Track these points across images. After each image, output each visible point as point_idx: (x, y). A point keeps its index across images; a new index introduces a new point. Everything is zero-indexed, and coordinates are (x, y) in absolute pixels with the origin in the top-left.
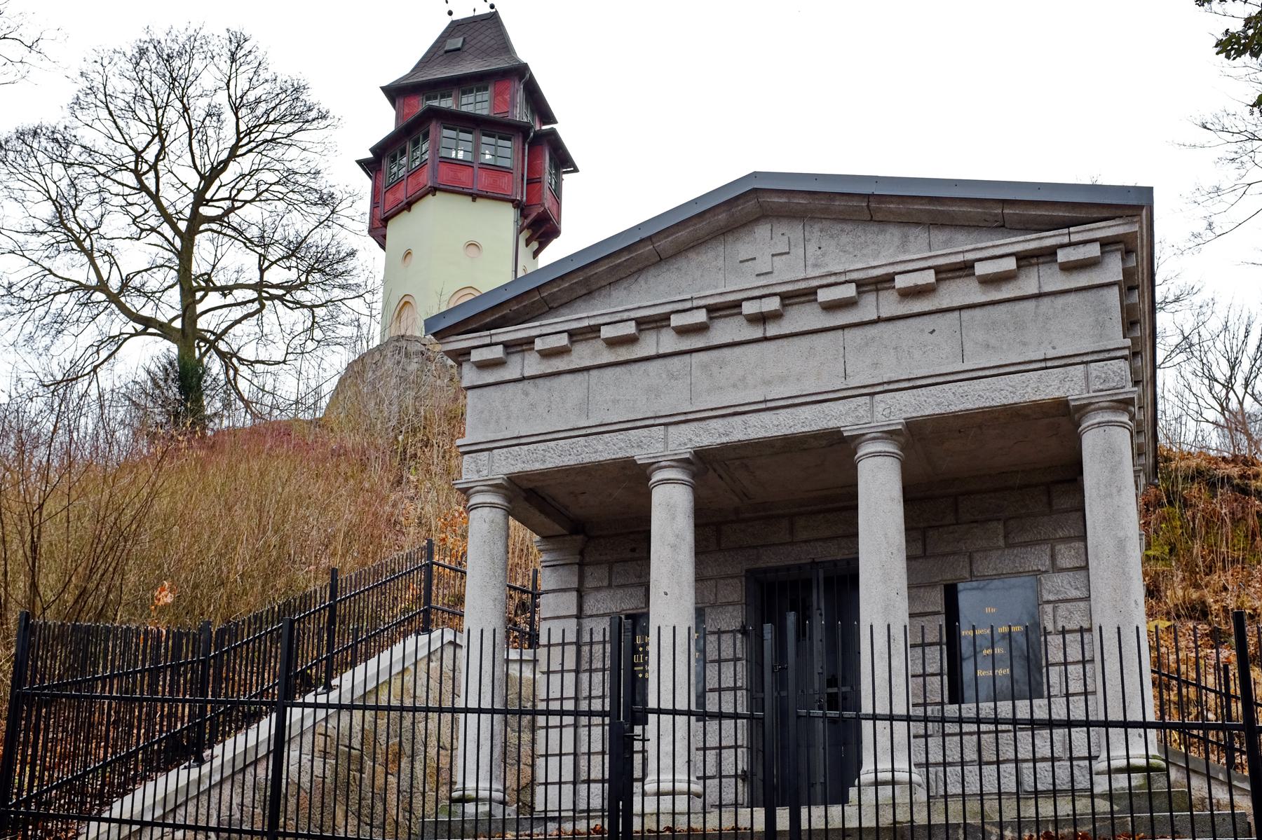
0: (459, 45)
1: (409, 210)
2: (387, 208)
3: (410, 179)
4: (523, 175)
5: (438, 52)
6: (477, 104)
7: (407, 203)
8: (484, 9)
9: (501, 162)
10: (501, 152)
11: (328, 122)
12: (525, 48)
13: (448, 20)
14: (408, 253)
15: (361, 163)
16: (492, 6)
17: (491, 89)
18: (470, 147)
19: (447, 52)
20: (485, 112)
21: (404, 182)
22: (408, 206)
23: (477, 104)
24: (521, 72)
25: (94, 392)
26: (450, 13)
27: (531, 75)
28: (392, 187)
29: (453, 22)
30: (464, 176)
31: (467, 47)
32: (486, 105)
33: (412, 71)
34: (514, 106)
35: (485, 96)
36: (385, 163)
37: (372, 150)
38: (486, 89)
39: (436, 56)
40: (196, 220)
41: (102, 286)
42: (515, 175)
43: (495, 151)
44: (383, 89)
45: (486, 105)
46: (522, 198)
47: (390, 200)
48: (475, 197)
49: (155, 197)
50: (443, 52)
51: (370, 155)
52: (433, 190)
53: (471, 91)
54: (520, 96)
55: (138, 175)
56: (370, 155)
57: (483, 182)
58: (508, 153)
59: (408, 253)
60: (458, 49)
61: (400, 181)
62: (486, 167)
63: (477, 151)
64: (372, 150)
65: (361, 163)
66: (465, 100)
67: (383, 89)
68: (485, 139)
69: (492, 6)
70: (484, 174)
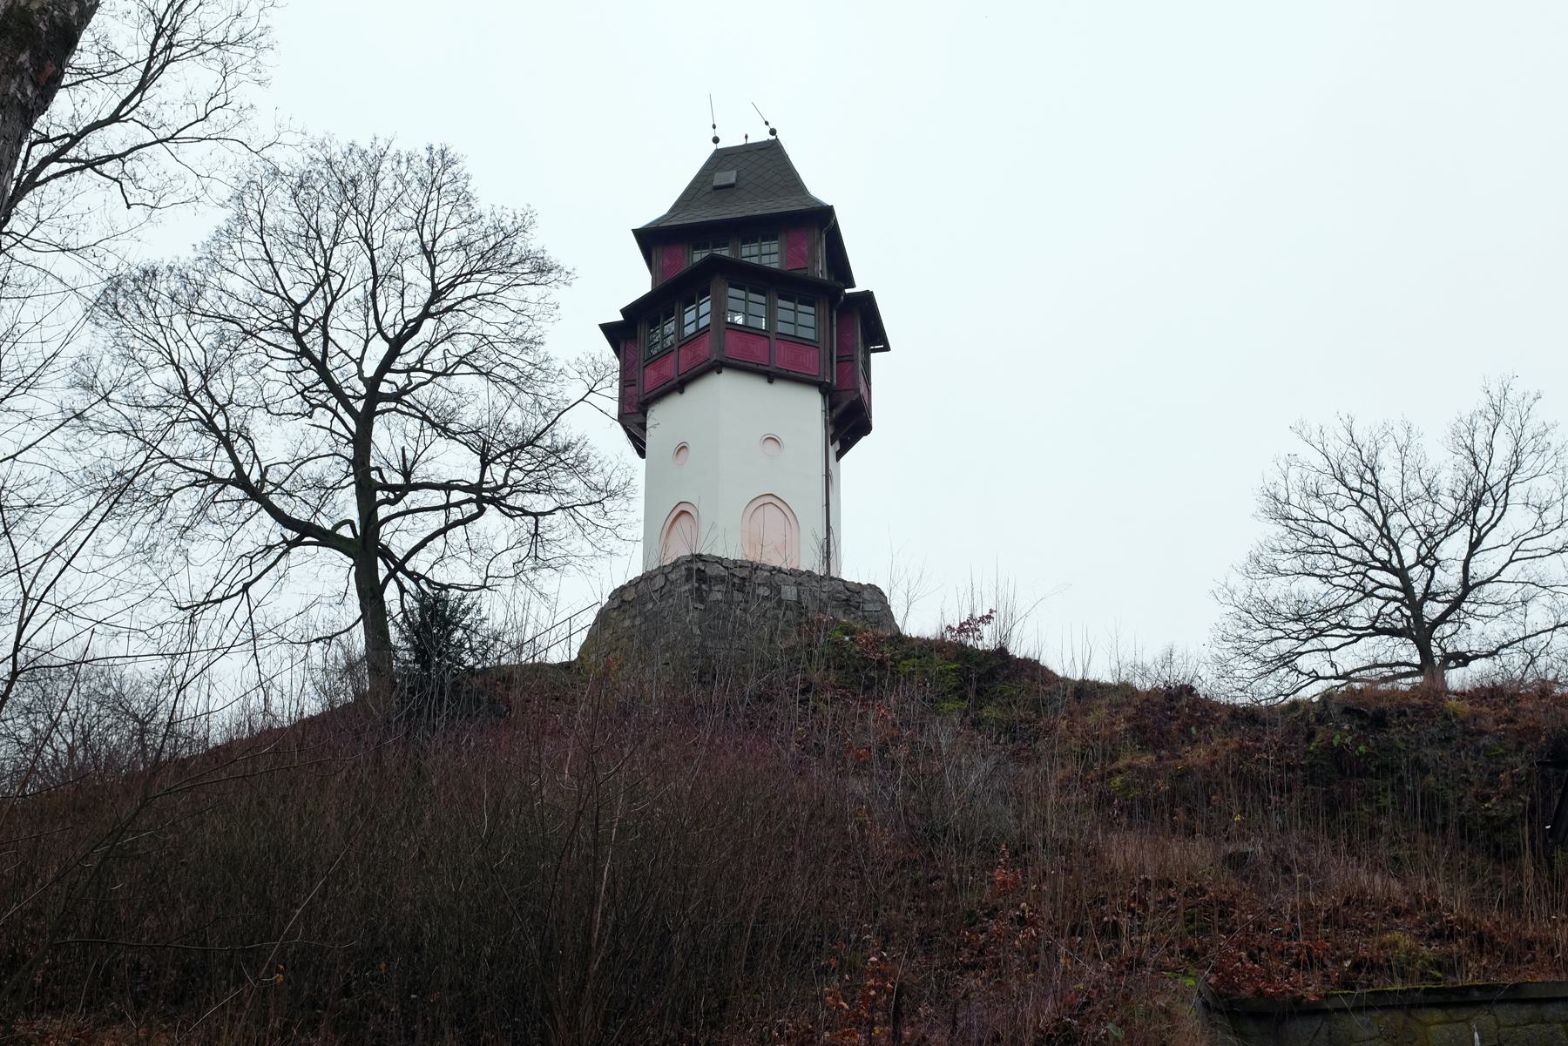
0: (733, 180)
1: (682, 392)
2: (648, 388)
3: (682, 351)
5: (702, 187)
6: (768, 255)
7: (680, 382)
8: (761, 136)
10: (802, 319)
11: (552, 276)
12: (820, 185)
13: (712, 148)
14: (683, 448)
15: (609, 330)
16: (773, 132)
18: (761, 310)
19: (717, 188)
20: (775, 266)
21: (673, 356)
22: (680, 386)
23: (768, 255)
24: (822, 219)
25: (242, 615)
26: (716, 140)
27: (836, 220)
28: (652, 361)
29: (717, 151)
30: (758, 351)
32: (775, 258)
33: (672, 210)
34: (815, 261)
35: (774, 247)
36: (642, 331)
37: (624, 311)
38: (774, 237)
40: (373, 396)
41: (241, 480)
42: (822, 349)
43: (801, 320)
44: (635, 231)
45: (775, 258)
46: (832, 381)
47: (651, 377)
48: (771, 377)
49: (321, 367)
50: (708, 188)
51: (620, 318)
52: (717, 367)
53: (754, 241)
54: (821, 253)
55: (298, 337)
56: (620, 318)
57: (783, 357)
58: (810, 321)
59: (683, 448)
60: (731, 186)
61: (666, 353)
62: (783, 338)
64: (624, 311)
66: (745, 251)
67: (635, 231)
68: (781, 303)
69: (773, 132)
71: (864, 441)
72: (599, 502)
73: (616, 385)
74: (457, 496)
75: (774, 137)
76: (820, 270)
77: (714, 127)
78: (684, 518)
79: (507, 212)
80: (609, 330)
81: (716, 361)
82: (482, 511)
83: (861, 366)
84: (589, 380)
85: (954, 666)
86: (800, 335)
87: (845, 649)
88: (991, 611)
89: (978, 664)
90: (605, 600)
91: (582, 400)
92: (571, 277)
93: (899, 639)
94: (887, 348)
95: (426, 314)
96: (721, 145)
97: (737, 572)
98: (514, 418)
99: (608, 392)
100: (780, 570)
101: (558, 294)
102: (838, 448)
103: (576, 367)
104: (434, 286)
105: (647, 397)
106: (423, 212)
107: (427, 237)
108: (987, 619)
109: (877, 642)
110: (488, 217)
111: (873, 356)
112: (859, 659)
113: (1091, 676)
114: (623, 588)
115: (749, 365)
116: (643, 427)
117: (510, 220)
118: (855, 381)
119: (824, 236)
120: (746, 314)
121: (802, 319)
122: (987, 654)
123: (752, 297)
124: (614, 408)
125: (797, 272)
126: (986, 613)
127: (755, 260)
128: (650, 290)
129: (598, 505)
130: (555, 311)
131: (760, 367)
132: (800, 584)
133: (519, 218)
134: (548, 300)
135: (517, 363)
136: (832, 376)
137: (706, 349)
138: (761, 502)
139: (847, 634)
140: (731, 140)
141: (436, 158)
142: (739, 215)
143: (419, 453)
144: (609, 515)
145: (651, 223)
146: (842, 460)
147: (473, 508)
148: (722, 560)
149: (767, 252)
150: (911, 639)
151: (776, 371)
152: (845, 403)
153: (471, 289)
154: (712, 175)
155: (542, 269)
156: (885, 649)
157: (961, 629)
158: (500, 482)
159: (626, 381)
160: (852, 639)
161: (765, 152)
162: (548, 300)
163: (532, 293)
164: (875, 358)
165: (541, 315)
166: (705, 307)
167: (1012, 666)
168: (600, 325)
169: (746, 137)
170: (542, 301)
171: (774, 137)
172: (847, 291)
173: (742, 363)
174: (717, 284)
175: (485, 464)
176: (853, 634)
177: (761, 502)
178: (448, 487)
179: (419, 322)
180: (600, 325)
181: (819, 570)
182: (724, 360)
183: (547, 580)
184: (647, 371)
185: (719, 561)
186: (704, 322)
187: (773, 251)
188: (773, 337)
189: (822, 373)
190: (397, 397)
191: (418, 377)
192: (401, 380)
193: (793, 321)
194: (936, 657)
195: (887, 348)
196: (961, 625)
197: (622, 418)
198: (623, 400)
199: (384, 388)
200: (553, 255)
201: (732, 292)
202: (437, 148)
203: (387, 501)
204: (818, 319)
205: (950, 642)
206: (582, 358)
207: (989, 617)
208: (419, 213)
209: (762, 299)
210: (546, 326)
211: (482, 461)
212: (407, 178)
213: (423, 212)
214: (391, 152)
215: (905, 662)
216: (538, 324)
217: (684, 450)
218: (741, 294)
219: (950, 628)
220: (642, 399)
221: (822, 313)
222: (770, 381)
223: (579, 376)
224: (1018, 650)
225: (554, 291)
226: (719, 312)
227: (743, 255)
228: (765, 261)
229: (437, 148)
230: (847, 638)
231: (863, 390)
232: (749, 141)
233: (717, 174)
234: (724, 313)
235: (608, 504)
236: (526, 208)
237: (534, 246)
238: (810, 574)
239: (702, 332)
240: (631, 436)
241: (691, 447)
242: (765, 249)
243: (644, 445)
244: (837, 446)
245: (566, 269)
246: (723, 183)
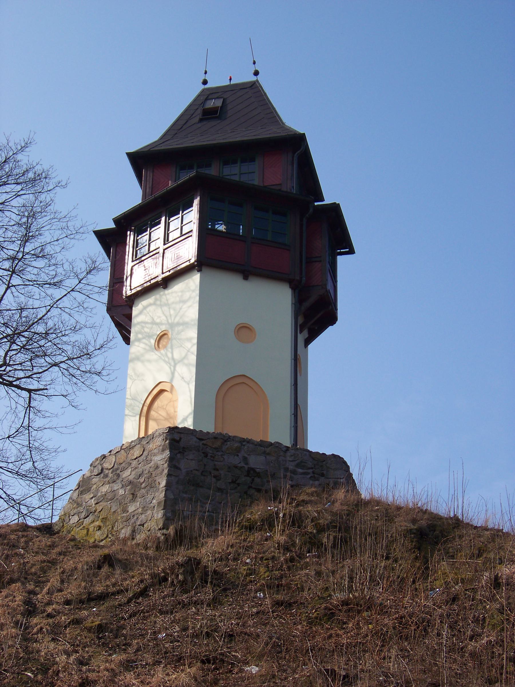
4: (301, 255)
7: (163, 279)
20: (256, 183)
29: (203, 91)
38: (252, 160)
44: (129, 155)
51: (113, 226)
53: (235, 162)
56: (113, 226)
64: (117, 221)
67: (129, 155)
83: (328, 266)
94: (352, 252)
96: (207, 86)
102: (307, 336)
111: (339, 258)
116: (129, 317)
119: (295, 158)
127: (236, 178)
128: (141, 202)
132: (269, 454)
136: (301, 273)
145: (141, 149)
152: (313, 298)
164: (342, 260)
169: (230, 79)
172: (316, 204)
181: (286, 441)
195: (352, 252)
222: (246, 278)
227: (224, 174)
228: (244, 179)
231: (330, 287)
238: (277, 446)
240: (118, 325)
243: (129, 332)
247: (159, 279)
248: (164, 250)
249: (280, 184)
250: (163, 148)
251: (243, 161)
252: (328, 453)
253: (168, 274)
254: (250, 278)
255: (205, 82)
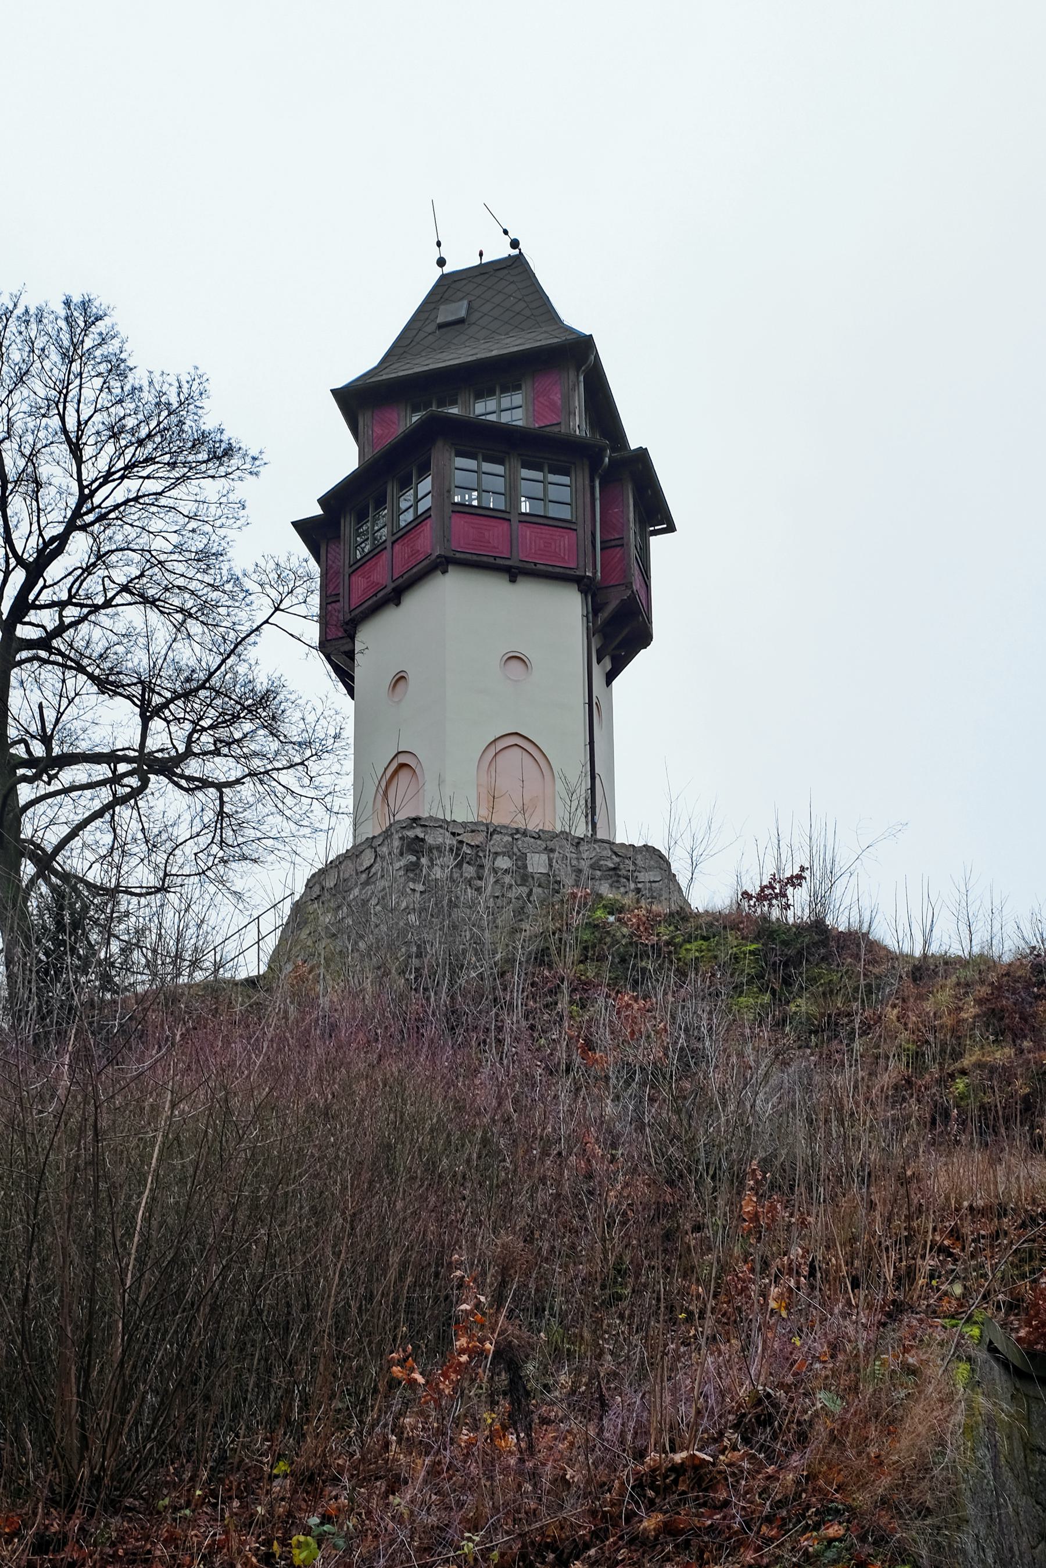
0: (463, 313)
1: (398, 604)
3: (397, 547)
7: (394, 589)
9: (555, 511)
11: (235, 462)
13: (438, 272)
14: (400, 679)
15: (304, 528)
16: (515, 244)
17: (527, 386)
18: (499, 484)
19: (441, 326)
20: (520, 423)
21: (386, 555)
22: (395, 596)
29: (443, 277)
31: (476, 316)
34: (570, 413)
35: (518, 399)
36: (347, 526)
37: (323, 501)
38: (517, 388)
39: (422, 335)
42: (580, 531)
45: (518, 414)
46: (595, 573)
47: (360, 588)
48: (514, 573)
50: (431, 327)
51: (317, 511)
52: (442, 564)
53: (491, 393)
56: (317, 511)
58: (565, 494)
59: (400, 679)
60: (461, 321)
62: (527, 519)
63: (512, 495)
64: (323, 501)
65: (301, 526)
66: (480, 408)
68: (525, 473)
69: (515, 244)
70: (528, 532)
71: (642, 658)
72: (302, 763)
73: (315, 599)
74: (122, 768)
75: (517, 251)
76: (578, 425)
77: (439, 244)
78: (404, 775)
79: (169, 379)
80: (304, 528)
81: (438, 557)
82: (145, 783)
84: (274, 594)
85: (753, 947)
86: (550, 515)
87: (608, 933)
88: (802, 869)
89: (784, 943)
90: (300, 889)
91: (266, 622)
92: (257, 463)
93: (683, 915)
95: (72, 526)
96: (448, 269)
97: (466, 838)
98: (187, 654)
99: (302, 610)
100: (525, 833)
101: (245, 489)
103: (255, 577)
104: (81, 487)
105: (353, 614)
106: (64, 391)
107: (71, 424)
108: (796, 880)
109: (652, 922)
110: (146, 388)
112: (626, 946)
113: (934, 949)
114: (322, 872)
115: (485, 559)
116: (351, 655)
117: (174, 390)
118: (626, 572)
119: (582, 378)
120: (481, 491)
121: (554, 493)
122: (800, 929)
123: (487, 467)
124: (312, 632)
125: (548, 429)
126: (797, 871)
127: (492, 418)
129: (300, 768)
130: (242, 513)
131: (499, 561)
133: (185, 386)
134: (232, 497)
135: (193, 585)
137: (429, 543)
138: (501, 745)
139: (611, 913)
140: (461, 260)
141: (76, 314)
142: (470, 359)
143: (61, 710)
144: (317, 781)
146: (615, 683)
147: (134, 781)
148: (448, 823)
149: (509, 406)
150: (698, 915)
151: (520, 565)
153: (131, 486)
154: (436, 308)
155: (222, 454)
156: (662, 929)
157: (761, 897)
158: (181, 748)
159: (328, 598)
160: (619, 920)
161: (506, 271)
162: (232, 497)
163: (211, 489)
165: (223, 520)
166: (425, 485)
167: (833, 944)
168: (296, 524)
169: (481, 254)
170: (224, 500)
171: (517, 251)
173: (475, 558)
174: (441, 454)
175: (146, 717)
176: (620, 912)
177: (501, 745)
178: (111, 758)
179: (62, 539)
180: (296, 524)
181: (581, 830)
182: (451, 554)
183: (240, 876)
184: (354, 578)
185: (443, 824)
186: (423, 507)
187: (515, 404)
188: (515, 519)
189: (582, 564)
190: (43, 643)
191: (71, 613)
192: (48, 618)
193: (542, 496)
194: (731, 938)
196: (762, 890)
197: (325, 646)
198: (324, 619)
199: (23, 632)
200: (234, 433)
201: (460, 462)
202: (76, 299)
203: (25, 779)
204: (574, 493)
205: (748, 915)
206: (262, 563)
207: (800, 877)
208: (60, 393)
209: (499, 469)
210: (232, 534)
211: (142, 715)
212: (39, 344)
213: (64, 391)
214: (19, 311)
215: (688, 946)
216: (222, 532)
217: (402, 683)
218: (472, 464)
219: (746, 895)
220: (348, 617)
221: (580, 480)
222: (513, 580)
223: (260, 589)
224: (840, 920)
225: (237, 484)
226: (442, 492)
227: (477, 412)
228: (505, 418)
229: (76, 299)
230: (611, 919)
232: (485, 260)
233: (442, 307)
234: (449, 491)
235: (314, 767)
236: (193, 372)
237: (208, 424)
239: (421, 519)
240: (337, 669)
241: (411, 677)
242: (506, 401)
243: (352, 679)
244: (607, 663)
245: (254, 452)
246: (451, 318)
247: (389, 589)
248: (393, 543)
249: (559, 424)
250: (384, 377)
251: (505, 389)
252: (639, 843)
253: (400, 580)
254: (519, 578)
255: (441, 262)
